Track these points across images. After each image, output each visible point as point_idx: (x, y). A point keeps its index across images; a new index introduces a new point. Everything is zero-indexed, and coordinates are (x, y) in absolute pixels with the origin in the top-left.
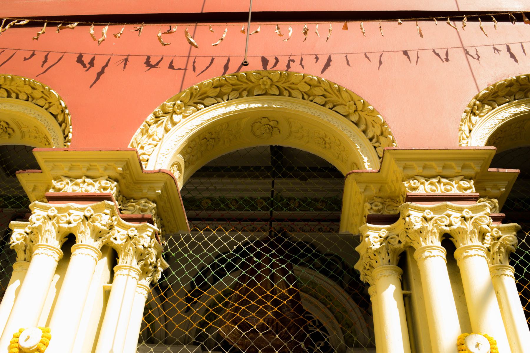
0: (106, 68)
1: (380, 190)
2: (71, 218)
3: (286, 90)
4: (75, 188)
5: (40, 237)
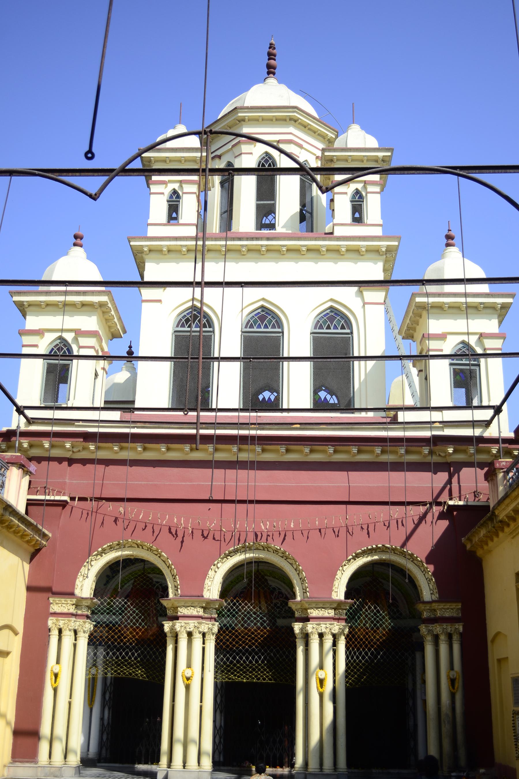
0: (184, 538)
1: (301, 606)
3: (266, 548)
4: (188, 612)
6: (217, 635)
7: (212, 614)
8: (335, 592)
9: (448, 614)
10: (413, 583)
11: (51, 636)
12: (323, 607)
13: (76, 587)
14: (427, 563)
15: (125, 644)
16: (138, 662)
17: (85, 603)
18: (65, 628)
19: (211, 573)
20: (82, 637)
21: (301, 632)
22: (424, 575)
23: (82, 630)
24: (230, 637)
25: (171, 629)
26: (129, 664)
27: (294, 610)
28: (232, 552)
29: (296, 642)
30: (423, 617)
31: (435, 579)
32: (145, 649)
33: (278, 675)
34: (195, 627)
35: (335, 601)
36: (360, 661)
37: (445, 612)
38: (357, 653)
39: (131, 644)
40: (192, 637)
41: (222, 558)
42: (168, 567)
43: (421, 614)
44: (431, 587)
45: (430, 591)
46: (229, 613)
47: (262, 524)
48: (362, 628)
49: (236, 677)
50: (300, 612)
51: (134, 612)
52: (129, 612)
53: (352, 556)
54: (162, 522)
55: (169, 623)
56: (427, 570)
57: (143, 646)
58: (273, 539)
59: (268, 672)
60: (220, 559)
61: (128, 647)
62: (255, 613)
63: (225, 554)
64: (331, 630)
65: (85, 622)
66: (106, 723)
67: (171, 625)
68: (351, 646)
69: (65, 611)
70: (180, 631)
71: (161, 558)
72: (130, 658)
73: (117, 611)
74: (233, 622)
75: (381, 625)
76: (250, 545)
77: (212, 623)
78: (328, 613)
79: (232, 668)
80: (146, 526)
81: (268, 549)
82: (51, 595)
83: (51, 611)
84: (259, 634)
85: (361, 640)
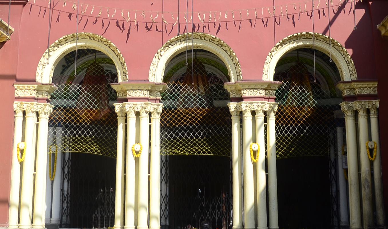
1: (235, 88)
2: (138, 107)
3: (203, 37)
5: (129, 114)
6: (161, 114)
7: (156, 96)
8: (265, 75)
9: (366, 92)
10: (334, 67)
11: (16, 118)
12: (255, 88)
13: (37, 74)
14: (346, 48)
15: (80, 124)
16: (93, 139)
17: (45, 88)
18: (28, 110)
19: (155, 60)
20: (43, 118)
21: (236, 110)
22: (344, 58)
23: (43, 112)
24: (173, 116)
25: (121, 109)
26: (85, 141)
27: (229, 91)
28: (173, 42)
29: (231, 120)
30: (344, 95)
31: (354, 62)
32: (99, 128)
33: (216, 149)
34: (143, 107)
35: (265, 83)
36: (289, 135)
37: (364, 91)
38: (286, 129)
39: (86, 124)
40: (140, 117)
41: (165, 47)
42: (117, 56)
43: (342, 92)
44: (351, 69)
45: (350, 72)
46: (171, 96)
47: (199, 16)
48: (289, 106)
49: (179, 151)
50: (235, 93)
51: (88, 96)
52: (83, 96)
53: (280, 42)
54: (111, 16)
55: (119, 105)
56: (347, 54)
57: (96, 125)
58: (209, 30)
59: (207, 147)
60: (162, 48)
61: (83, 126)
62: (194, 95)
63: (167, 43)
64: (262, 108)
65: (45, 105)
66: (65, 193)
67: (121, 106)
68: (280, 122)
69: (28, 95)
70: (129, 111)
71: (111, 48)
72: (85, 136)
73: (73, 95)
74: (175, 103)
75: (306, 103)
76: (189, 35)
77: (157, 104)
78: (260, 93)
79: (175, 143)
80: (96, 20)
81: (204, 38)
82: (15, 82)
83: (16, 96)
84: (198, 113)
85: (289, 117)
